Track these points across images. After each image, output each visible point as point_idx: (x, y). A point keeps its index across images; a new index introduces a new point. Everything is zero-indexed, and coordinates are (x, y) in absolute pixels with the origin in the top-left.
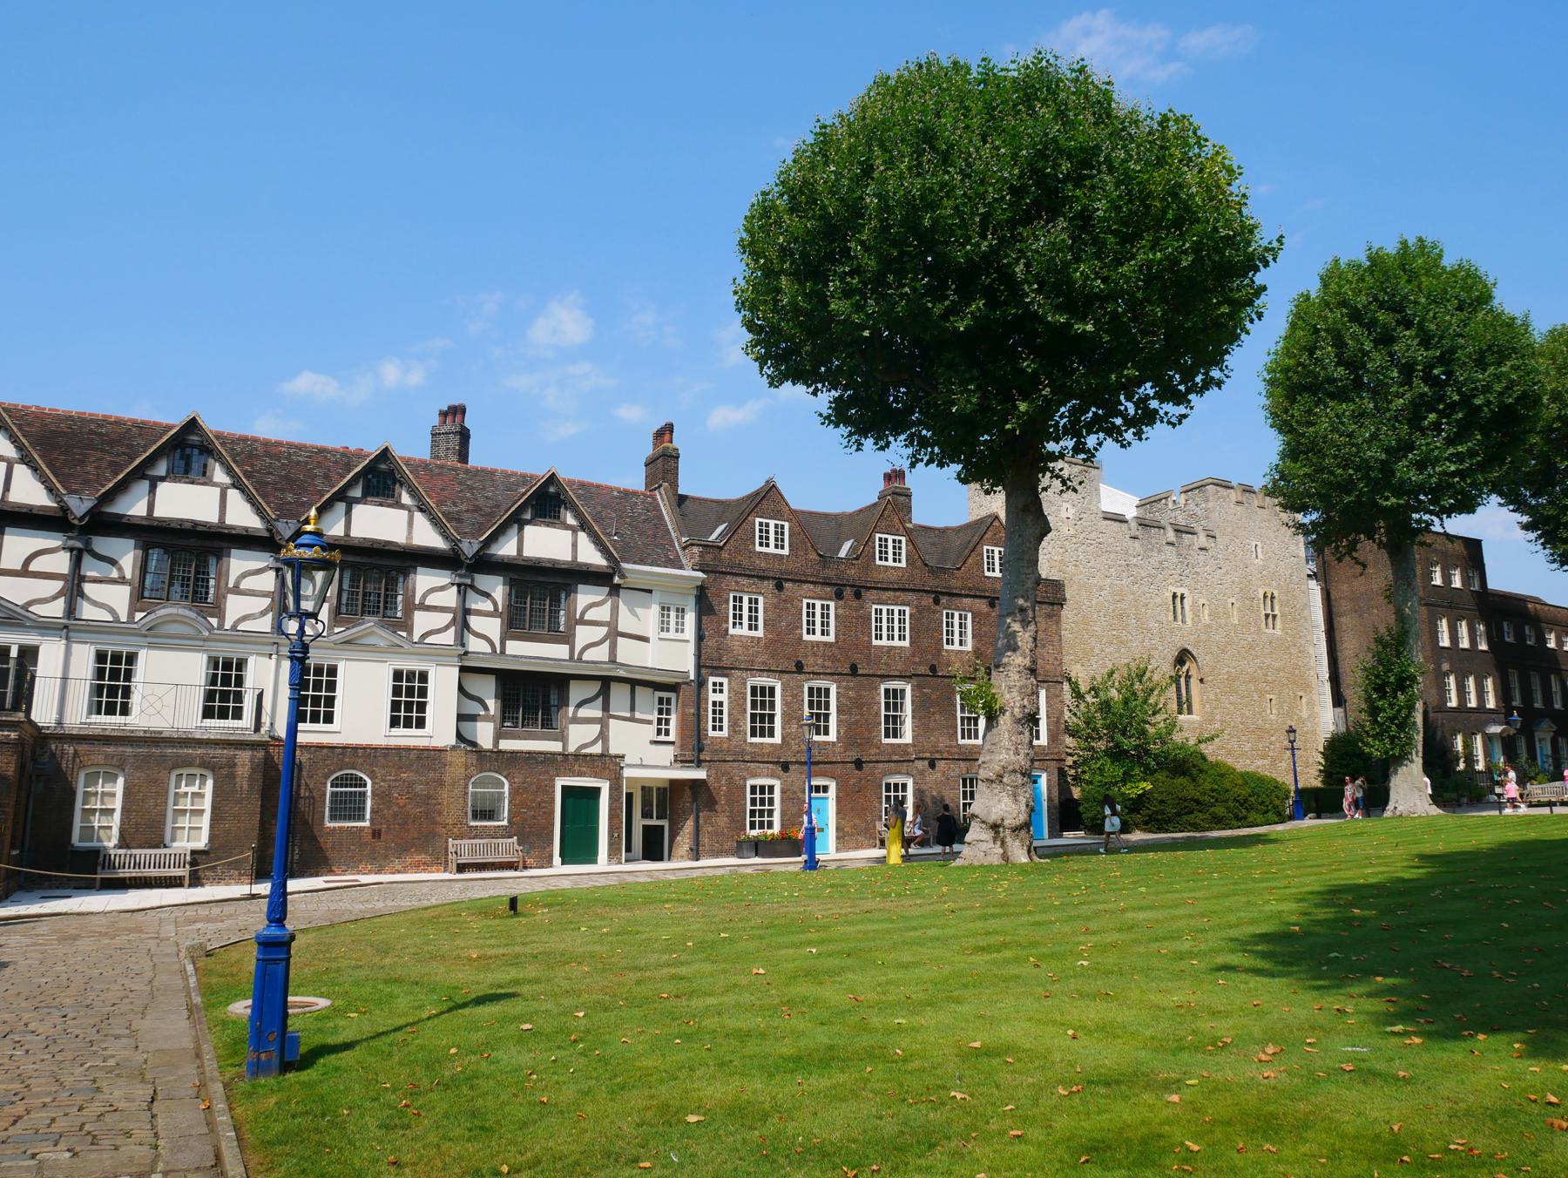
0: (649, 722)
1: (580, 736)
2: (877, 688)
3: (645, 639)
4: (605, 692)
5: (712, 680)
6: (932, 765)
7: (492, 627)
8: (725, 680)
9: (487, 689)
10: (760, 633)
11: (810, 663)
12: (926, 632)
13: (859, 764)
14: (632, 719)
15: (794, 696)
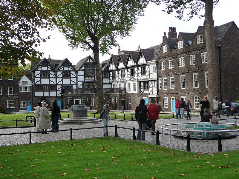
0: (156, 87)
1: (150, 90)
2: (179, 77)
3: (152, 73)
4: (152, 83)
5: (160, 79)
6: (188, 93)
7: (140, 75)
8: (160, 79)
9: (142, 84)
10: (164, 69)
11: (171, 73)
12: (187, 62)
13: (177, 94)
14: (155, 87)
15: (169, 81)
